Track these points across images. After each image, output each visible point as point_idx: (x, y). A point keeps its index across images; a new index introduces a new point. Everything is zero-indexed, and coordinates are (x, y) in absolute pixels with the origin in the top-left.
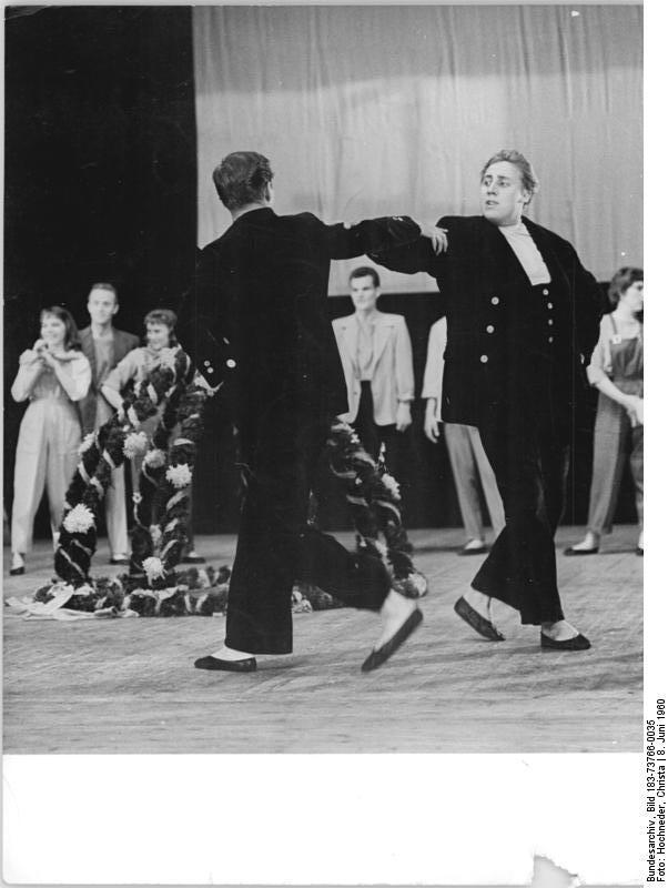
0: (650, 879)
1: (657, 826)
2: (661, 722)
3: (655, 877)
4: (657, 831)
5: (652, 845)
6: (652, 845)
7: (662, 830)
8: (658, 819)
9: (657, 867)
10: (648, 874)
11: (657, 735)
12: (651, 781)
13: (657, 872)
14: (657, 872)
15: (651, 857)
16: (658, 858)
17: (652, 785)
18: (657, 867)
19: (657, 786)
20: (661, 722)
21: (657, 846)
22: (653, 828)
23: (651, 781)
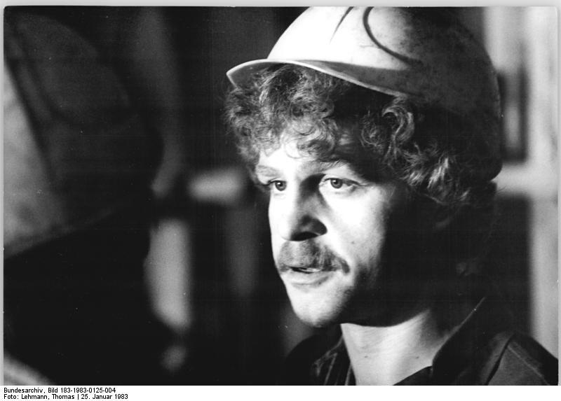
0: (5, 390)
1: (40, 394)
2: (113, 397)
3: (7, 393)
5: (27, 391)
6: (27, 391)
8: (43, 394)
9: (14, 394)
11: (97, 394)
13: (10, 394)
14: (10, 394)
15: (20, 391)
17: (65, 391)
18: (14, 394)
20: (113, 397)
21: (25, 394)
22: (38, 391)
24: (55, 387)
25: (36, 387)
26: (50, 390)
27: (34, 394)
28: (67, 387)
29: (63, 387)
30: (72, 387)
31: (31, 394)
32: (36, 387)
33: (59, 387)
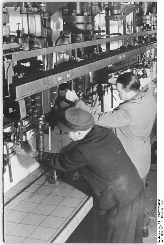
0: (159, 243)
3: (160, 242)
4: (161, 229)
5: (160, 233)
6: (160, 233)
7: (162, 231)
9: (161, 239)
10: (158, 241)
12: (159, 216)
13: (161, 241)
14: (161, 241)
15: (159, 236)
16: (161, 237)
17: (160, 216)
18: (161, 239)
19: (161, 216)
21: (161, 234)
23: (159, 216)
24: (158, 221)
25: (158, 229)
26: (159, 223)
27: (161, 230)
28: (158, 216)
29: (158, 217)
30: (158, 214)
31: (161, 231)
32: (158, 229)
33: (158, 219)
